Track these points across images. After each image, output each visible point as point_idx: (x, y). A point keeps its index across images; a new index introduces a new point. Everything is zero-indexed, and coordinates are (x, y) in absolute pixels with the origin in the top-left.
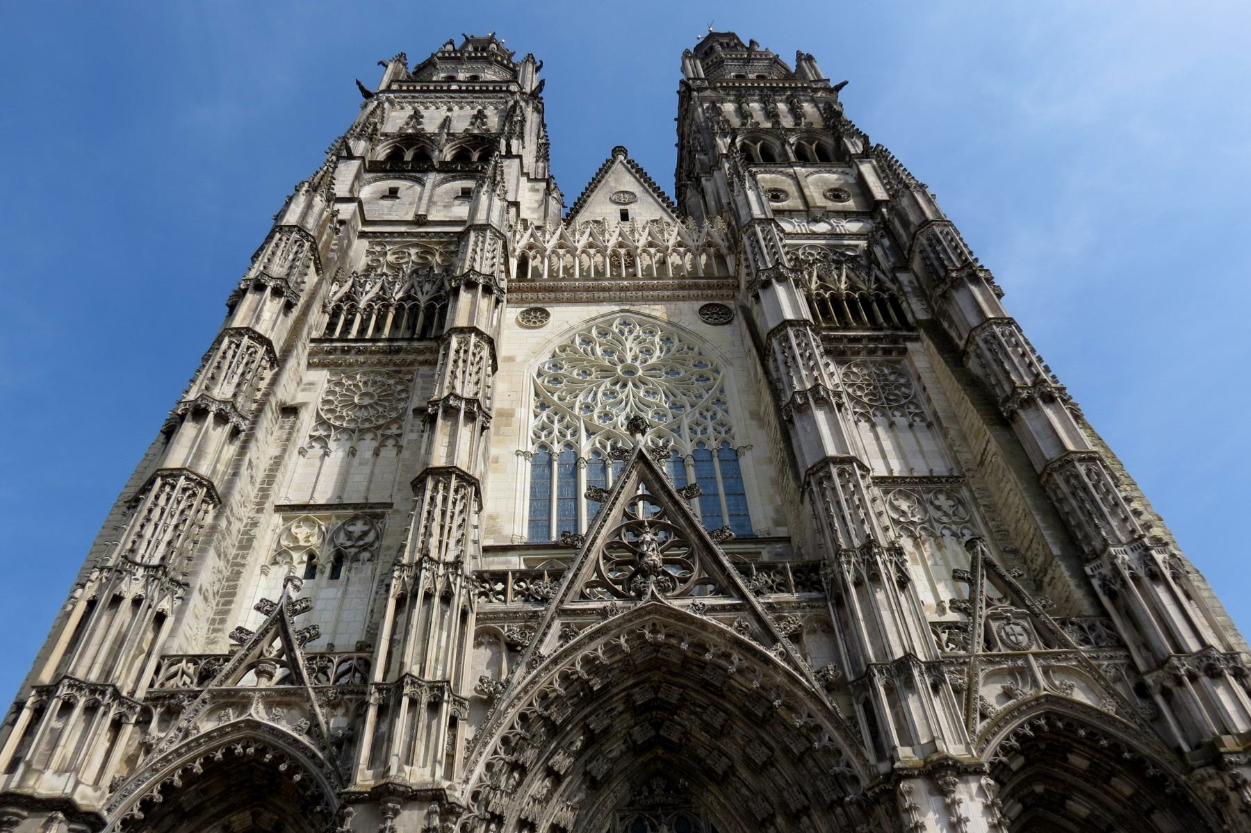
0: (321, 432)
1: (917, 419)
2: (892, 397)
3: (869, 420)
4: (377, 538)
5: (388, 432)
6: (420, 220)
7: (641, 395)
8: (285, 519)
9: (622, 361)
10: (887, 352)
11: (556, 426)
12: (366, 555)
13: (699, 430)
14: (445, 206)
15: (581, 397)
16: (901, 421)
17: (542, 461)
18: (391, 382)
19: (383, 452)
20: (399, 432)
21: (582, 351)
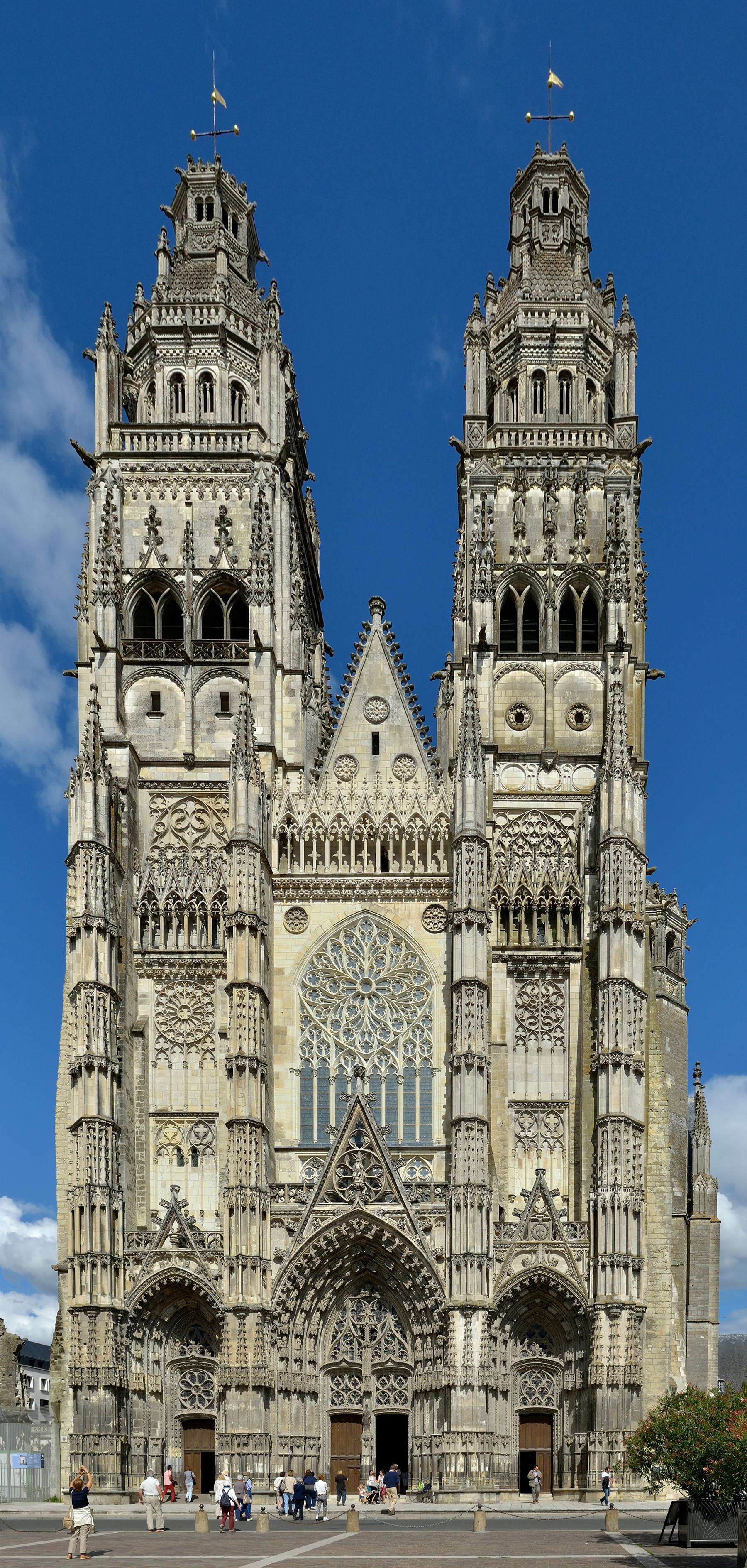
0: (162, 1044)
1: (558, 1043)
2: (548, 1021)
3: (525, 1044)
4: (214, 1138)
5: (205, 1046)
6: (190, 763)
7: (373, 1012)
8: (158, 1122)
9: (362, 970)
10: (555, 973)
11: (315, 1042)
12: (208, 1150)
13: (410, 1047)
14: (208, 730)
15: (331, 1014)
16: (546, 1044)
17: (305, 1074)
18: (199, 993)
19: (205, 1066)
20: (211, 1046)
21: (332, 959)
